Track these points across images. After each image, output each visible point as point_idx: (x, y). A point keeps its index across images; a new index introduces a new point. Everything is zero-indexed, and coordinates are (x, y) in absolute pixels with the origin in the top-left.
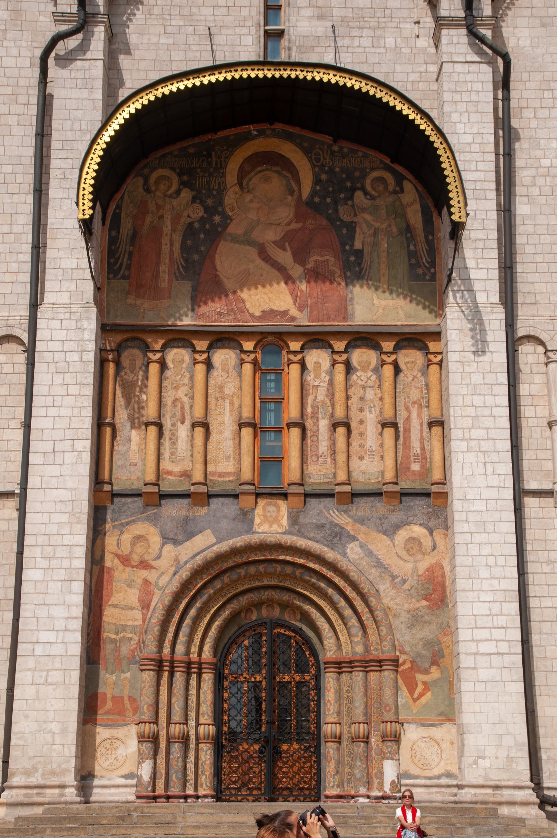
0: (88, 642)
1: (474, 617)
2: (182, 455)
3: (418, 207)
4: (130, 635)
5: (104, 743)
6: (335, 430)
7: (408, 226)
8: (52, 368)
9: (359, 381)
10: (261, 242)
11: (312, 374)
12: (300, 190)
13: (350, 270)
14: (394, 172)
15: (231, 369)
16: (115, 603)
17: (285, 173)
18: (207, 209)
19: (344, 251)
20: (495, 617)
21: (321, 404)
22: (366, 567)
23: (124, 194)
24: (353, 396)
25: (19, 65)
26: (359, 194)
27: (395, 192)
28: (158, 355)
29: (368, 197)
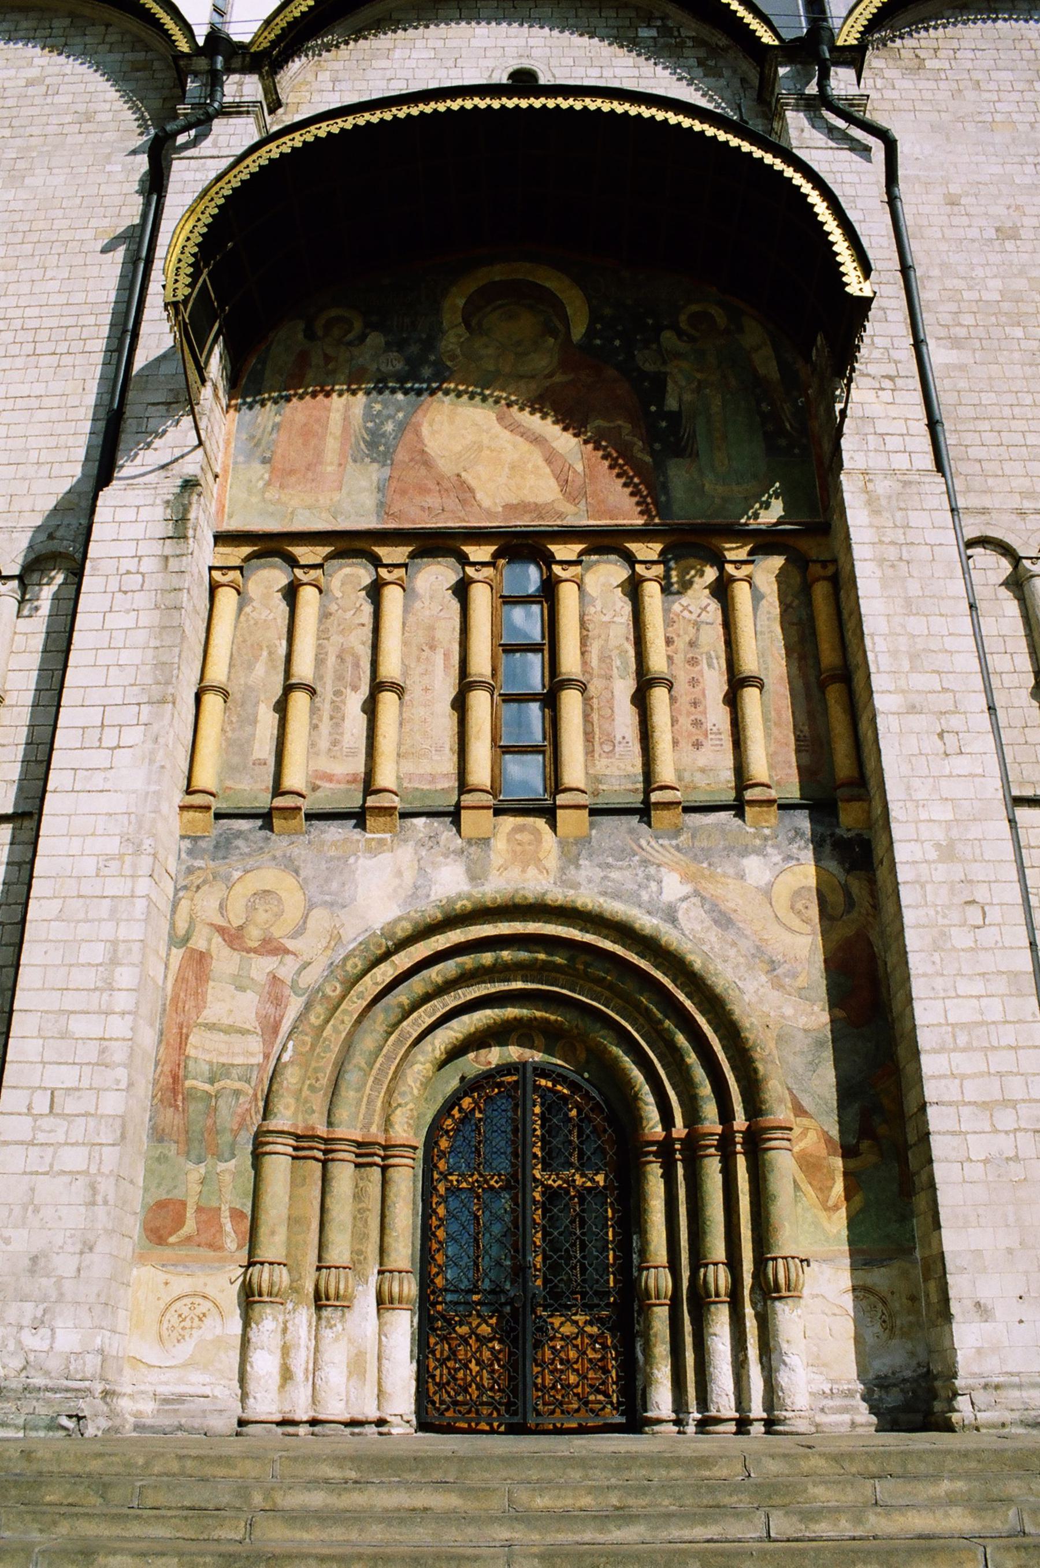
0: (153, 1097)
1: (950, 1029)
2: (352, 745)
3: (767, 351)
4: (238, 1085)
5: (178, 1304)
8: (113, 586)
9: (686, 613)
11: (599, 604)
12: (568, 328)
16: (212, 1020)
18: (408, 361)
20: (993, 1027)
22: (717, 947)
26: (668, 337)
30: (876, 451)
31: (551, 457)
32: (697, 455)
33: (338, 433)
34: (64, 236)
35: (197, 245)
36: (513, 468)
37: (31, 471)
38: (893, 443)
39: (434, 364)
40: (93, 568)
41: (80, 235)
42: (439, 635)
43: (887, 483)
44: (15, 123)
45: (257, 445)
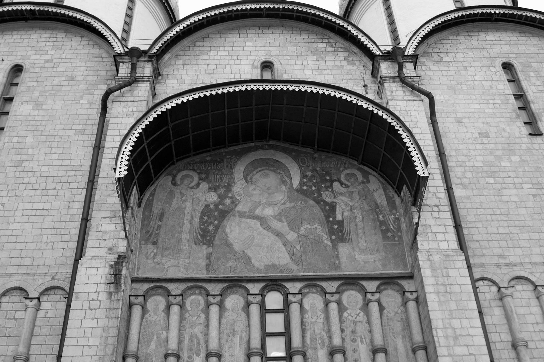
3: (381, 191)
6: (332, 357)
7: (376, 204)
8: (86, 306)
9: (350, 317)
10: (263, 216)
11: (309, 313)
13: (334, 234)
14: (360, 169)
15: (240, 311)
17: (279, 171)
18: (219, 196)
19: (328, 222)
21: (318, 336)
23: (156, 187)
24: (346, 329)
25: (89, 113)
26: (336, 185)
27: (363, 182)
28: (179, 299)
29: (344, 186)
30: (432, 241)
31: (285, 243)
32: (352, 241)
33: (188, 231)
34: (61, 133)
35: (130, 151)
36: (268, 248)
37: (44, 246)
38: (440, 237)
39: (231, 198)
40: (76, 297)
41: (68, 132)
42: (237, 329)
43: (438, 256)
44: (39, 79)
45: (150, 236)
